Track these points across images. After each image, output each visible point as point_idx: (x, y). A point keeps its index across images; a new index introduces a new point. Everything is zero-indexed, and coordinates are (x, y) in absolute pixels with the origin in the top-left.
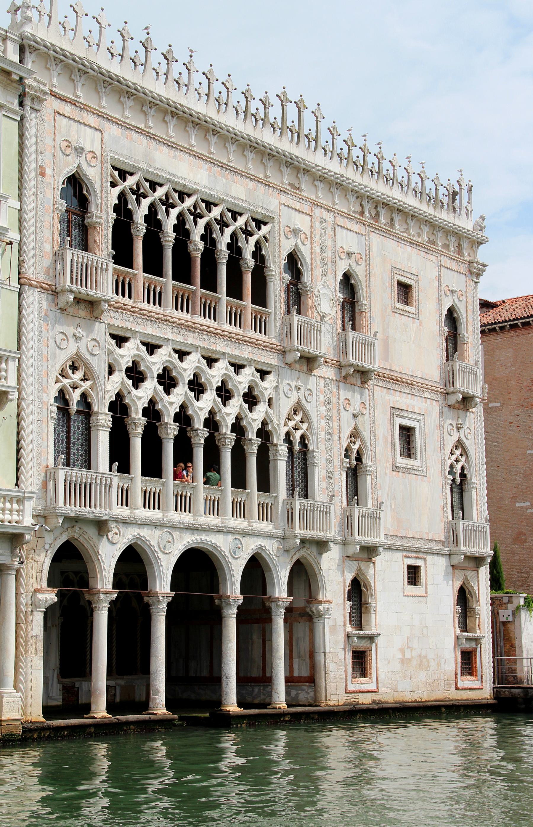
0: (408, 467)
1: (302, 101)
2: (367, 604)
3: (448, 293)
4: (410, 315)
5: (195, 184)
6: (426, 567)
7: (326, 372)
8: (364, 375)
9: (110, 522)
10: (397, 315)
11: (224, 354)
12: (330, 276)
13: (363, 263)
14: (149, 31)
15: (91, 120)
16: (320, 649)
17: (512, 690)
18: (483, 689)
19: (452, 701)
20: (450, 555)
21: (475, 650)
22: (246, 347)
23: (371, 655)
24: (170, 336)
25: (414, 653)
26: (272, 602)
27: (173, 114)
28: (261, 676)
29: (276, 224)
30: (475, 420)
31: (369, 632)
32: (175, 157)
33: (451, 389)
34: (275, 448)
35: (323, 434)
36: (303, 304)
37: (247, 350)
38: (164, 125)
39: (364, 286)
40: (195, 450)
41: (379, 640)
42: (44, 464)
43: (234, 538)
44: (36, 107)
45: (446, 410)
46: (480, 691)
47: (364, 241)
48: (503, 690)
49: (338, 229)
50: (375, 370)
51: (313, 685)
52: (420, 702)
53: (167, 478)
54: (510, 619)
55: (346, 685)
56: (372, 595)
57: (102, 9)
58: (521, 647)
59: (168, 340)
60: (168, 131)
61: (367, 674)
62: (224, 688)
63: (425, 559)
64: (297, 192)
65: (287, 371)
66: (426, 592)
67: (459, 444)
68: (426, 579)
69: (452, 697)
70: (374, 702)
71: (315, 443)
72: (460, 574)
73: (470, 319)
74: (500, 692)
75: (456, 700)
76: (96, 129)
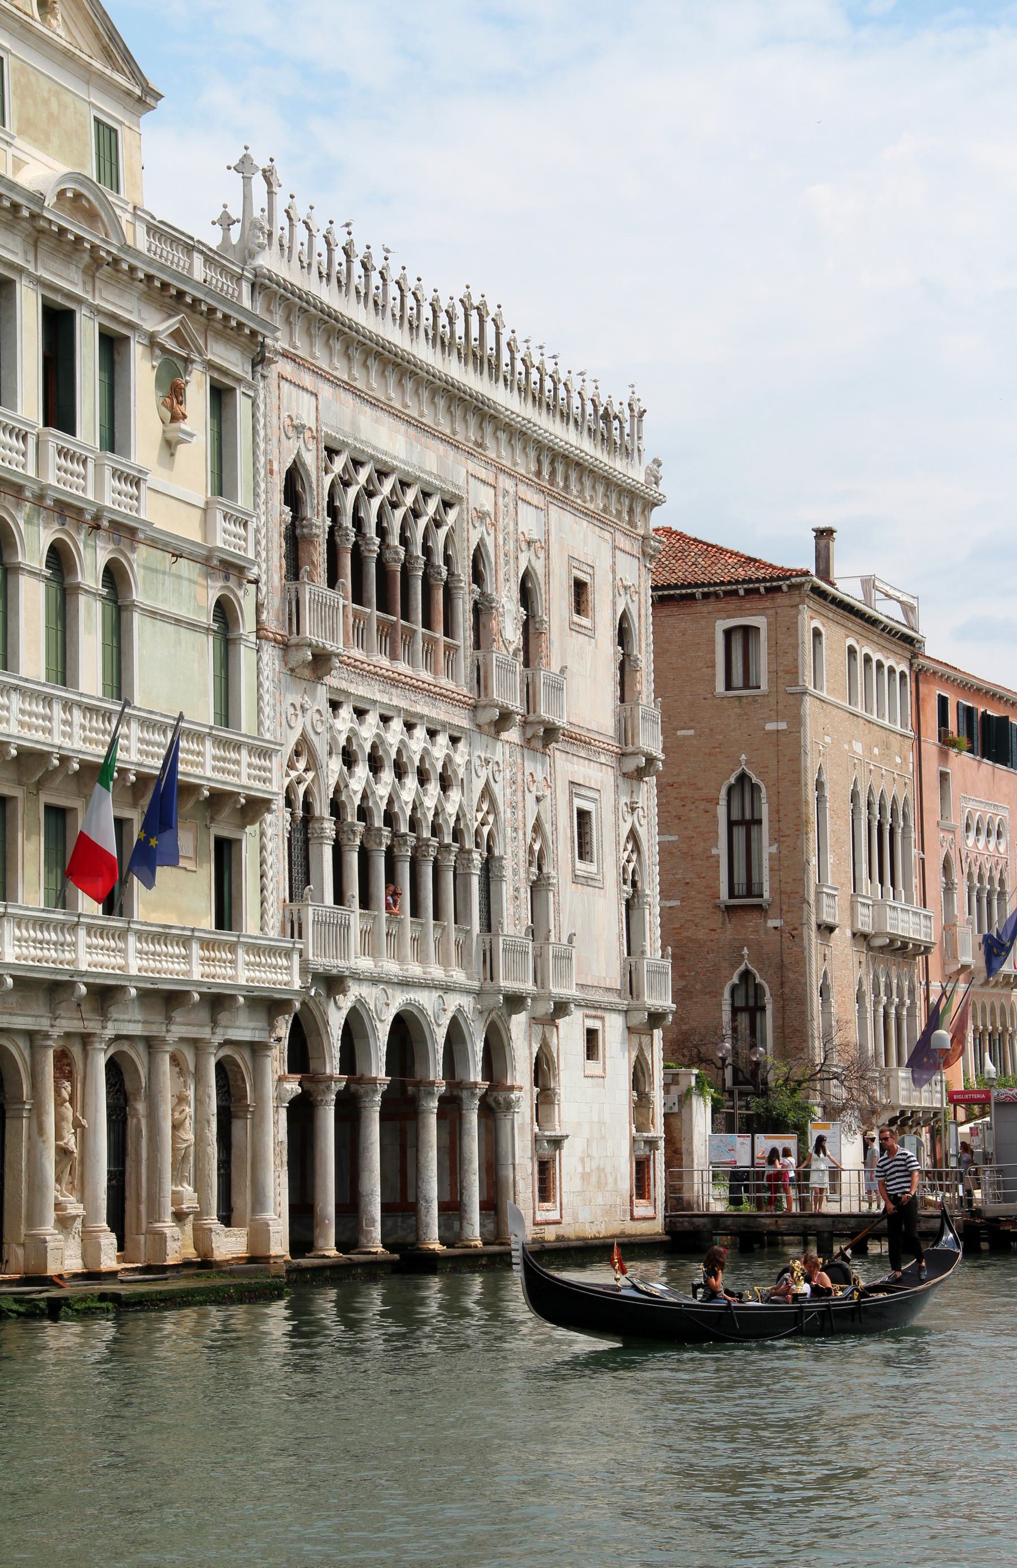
0: (586, 875)
1: (484, 304)
2: (549, 1089)
3: (622, 592)
4: (583, 631)
5: (395, 458)
6: (604, 1031)
7: (513, 735)
8: (551, 732)
9: (348, 979)
10: (574, 633)
11: (422, 717)
12: (513, 580)
13: (542, 555)
14: (351, 228)
15: (307, 380)
16: (507, 1160)
17: (695, 1219)
18: (654, 1218)
19: (627, 1236)
20: (626, 1012)
21: (648, 1159)
22: (440, 704)
23: (554, 1167)
24: (378, 697)
25: (594, 1166)
26: (462, 1089)
27: (378, 355)
28: (398, 1200)
29: (465, 507)
30: (648, 793)
31: (553, 1134)
32: (377, 421)
33: (630, 749)
34: (466, 856)
35: (509, 829)
36: (484, 627)
37: (394, 693)
38: (364, 372)
39: (543, 591)
40: (399, 865)
41: (566, 1144)
42: (282, 897)
43: (437, 995)
44: (266, 373)
45: (620, 779)
46: (651, 1222)
47: (543, 519)
48: (681, 1220)
49: (520, 502)
50: (563, 728)
51: (492, 1213)
52: (599, 1238)
53: (379, 909)
54: (676, 1109)
55: (534, 1213)
56: (554, 1077)
57: (312, 208)
58: (691, 1153)
59: (375, 702)
60: (368, 381)
61: (549, 1196)
62: (423, 1218)
63: (602, 1018)
64: (480, 450)
65: (476, 737)
66: (604, 1069)
67: (633, 835)
68: (604, 1050)
69: (628, 1231)
70: (559, 1238)
71: (502, 845)
72: (635, 1039)
73: (643, 631)
74: (675, 1223)
75: (631, 1236)
76: (312, 393)
